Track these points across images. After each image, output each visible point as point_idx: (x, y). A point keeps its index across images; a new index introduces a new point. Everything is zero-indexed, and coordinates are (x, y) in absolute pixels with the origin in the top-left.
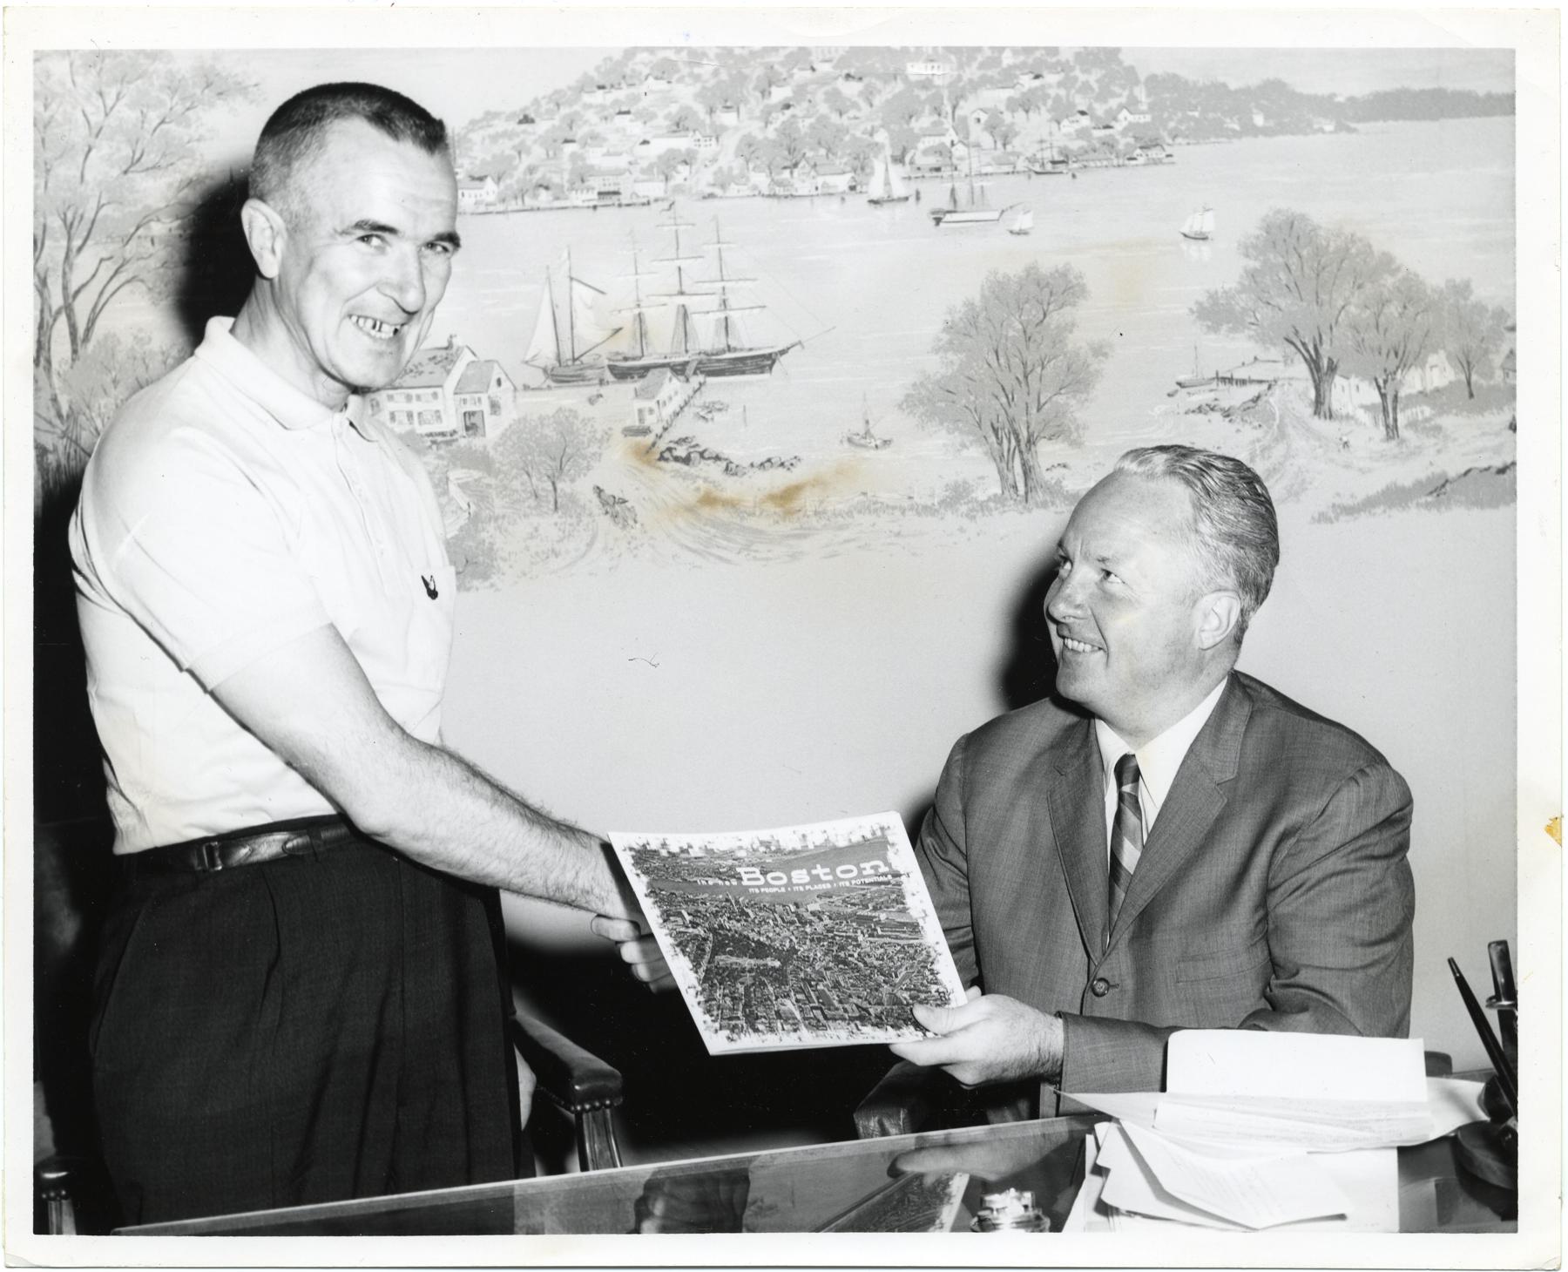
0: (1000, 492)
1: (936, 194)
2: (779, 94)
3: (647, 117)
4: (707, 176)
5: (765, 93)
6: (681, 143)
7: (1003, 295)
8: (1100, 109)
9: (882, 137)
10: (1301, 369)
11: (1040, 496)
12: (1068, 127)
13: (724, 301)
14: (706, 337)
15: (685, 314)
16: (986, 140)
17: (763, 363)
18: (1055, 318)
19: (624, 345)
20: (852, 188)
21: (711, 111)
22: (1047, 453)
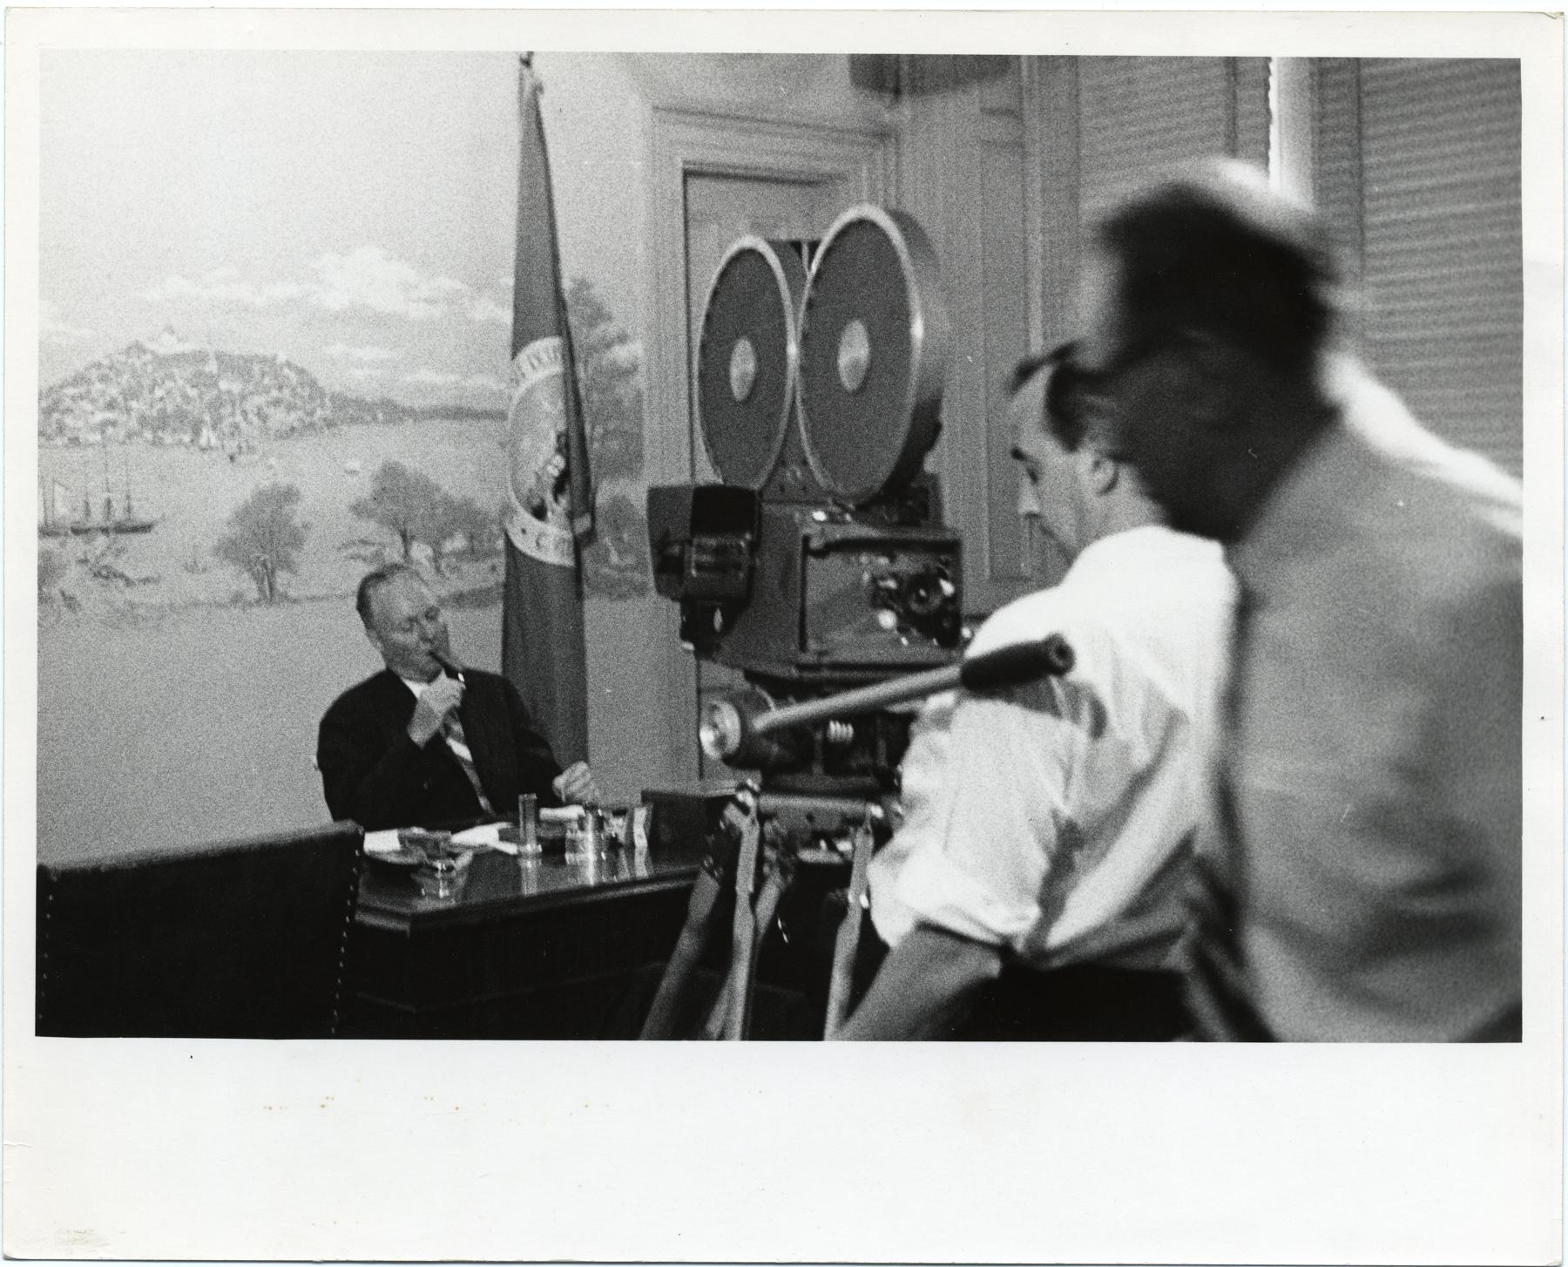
0: (256, 596)
1: (231, 445)
2: (159, 393)
3: (93, 401)
4: (122, 433)
5: (152, 391)
6: (110, 415)
7: (262, 497)
8: (308, 407)
9: (207, 418)
10: (398, 538)
11: (277, 599)
12: (293, 415)
13: (128, 497)
14: (119, 515)
15: (109, 502)
16: (255, 420)
17: (145, 528)
18: (287, 509)
19: (78, 516)
20: (192, 441)
21: (126, 400)
22: (282, 578)
